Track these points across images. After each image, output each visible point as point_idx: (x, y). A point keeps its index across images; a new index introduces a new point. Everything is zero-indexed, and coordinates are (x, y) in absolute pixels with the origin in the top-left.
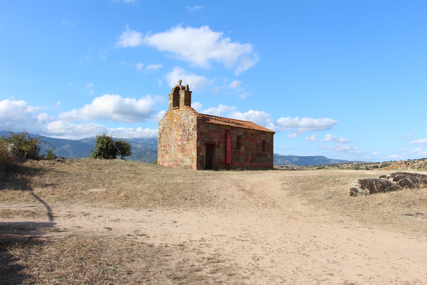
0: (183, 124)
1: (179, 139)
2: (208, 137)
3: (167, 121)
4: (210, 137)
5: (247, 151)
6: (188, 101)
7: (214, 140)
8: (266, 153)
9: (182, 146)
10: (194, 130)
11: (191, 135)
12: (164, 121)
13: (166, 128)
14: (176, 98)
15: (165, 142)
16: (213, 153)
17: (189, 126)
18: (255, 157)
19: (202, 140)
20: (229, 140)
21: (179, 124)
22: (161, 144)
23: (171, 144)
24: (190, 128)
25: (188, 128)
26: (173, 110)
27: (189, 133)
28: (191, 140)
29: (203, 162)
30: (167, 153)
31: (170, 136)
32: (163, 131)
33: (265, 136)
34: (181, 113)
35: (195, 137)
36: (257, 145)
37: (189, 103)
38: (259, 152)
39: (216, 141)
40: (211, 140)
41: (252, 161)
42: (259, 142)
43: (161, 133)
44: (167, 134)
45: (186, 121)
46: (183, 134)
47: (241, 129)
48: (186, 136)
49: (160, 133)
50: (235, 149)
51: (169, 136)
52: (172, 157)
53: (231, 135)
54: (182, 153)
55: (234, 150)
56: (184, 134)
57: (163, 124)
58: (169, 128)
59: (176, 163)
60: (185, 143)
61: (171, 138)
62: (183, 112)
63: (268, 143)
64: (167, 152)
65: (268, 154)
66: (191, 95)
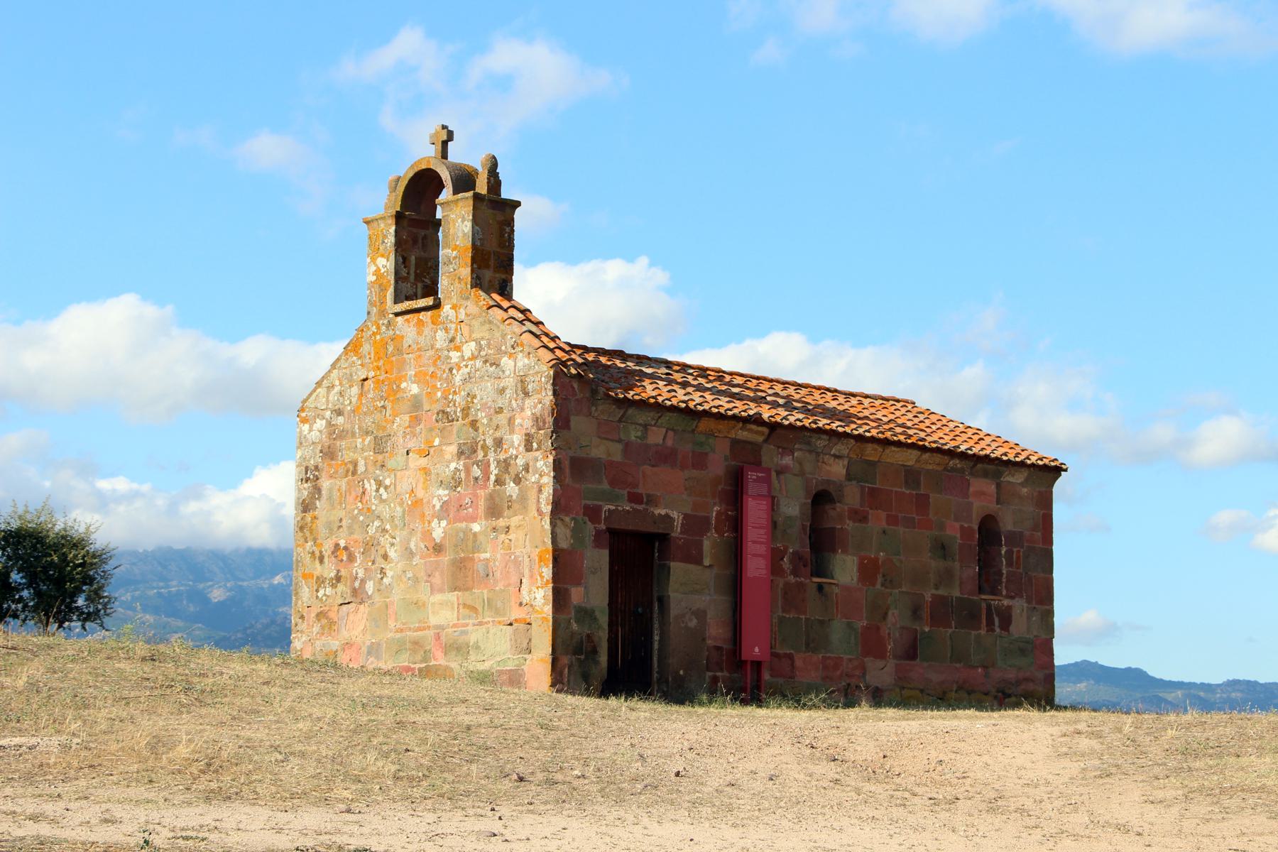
0: (466, 411)
1: (438, 507)
2: (625, 492)
3: (355, 390)
4: (639, 491)
5: (878, 586)
6: (492, 263)
7: (663, 512)
8: (1006, 602)
9: (456, 546)
10: (535, 445)
11: (517, 480)
12: (337, 389)
13: (353, 435)
14: (415, 241)
15: (344, 523)
16: (655, 595)
17: (502, 419)
18: (927, 629)
19: (587, 508)
20: (755, 511)
21: (437, 407)
22: (315, 540)
23: (385, 541)
24: (512, 432)
25: (498, 434)
26: (399, 319)
27: (505, 465)
28: (516, 506)
29: (595, 651)
30: (358, 595)
31: (379, 484)
32: (329, 454)
33: (993, 487)
34: (452, 340)
35: (540, 491)
36: (942, 549)
37: (503, 276)
38: (956, 593)
39: (675, 515)
40: (640, 507)
41: (911, 652)
42: (953, 531)
43: (316, 468)
44: (354, 473)
45: (485, 392)
46: (463, 475)
47: (834, 439)
48: (485, 487)
49: (307, 469)
50: (795, 572)
51: (370, 486)
52: (391, 624)
53: (767, 480)
54: (453, 597)
55: (792, 579)
56: (468, 470)
57: (328, 414)
58: (367, 433)
59: (419, 657)
60: (476, 527)
61: (382, 501)
62: (465, 329)
63: (1015, 539)
64: (355, 592)
65: (1019, 606)
66: (510, 223)
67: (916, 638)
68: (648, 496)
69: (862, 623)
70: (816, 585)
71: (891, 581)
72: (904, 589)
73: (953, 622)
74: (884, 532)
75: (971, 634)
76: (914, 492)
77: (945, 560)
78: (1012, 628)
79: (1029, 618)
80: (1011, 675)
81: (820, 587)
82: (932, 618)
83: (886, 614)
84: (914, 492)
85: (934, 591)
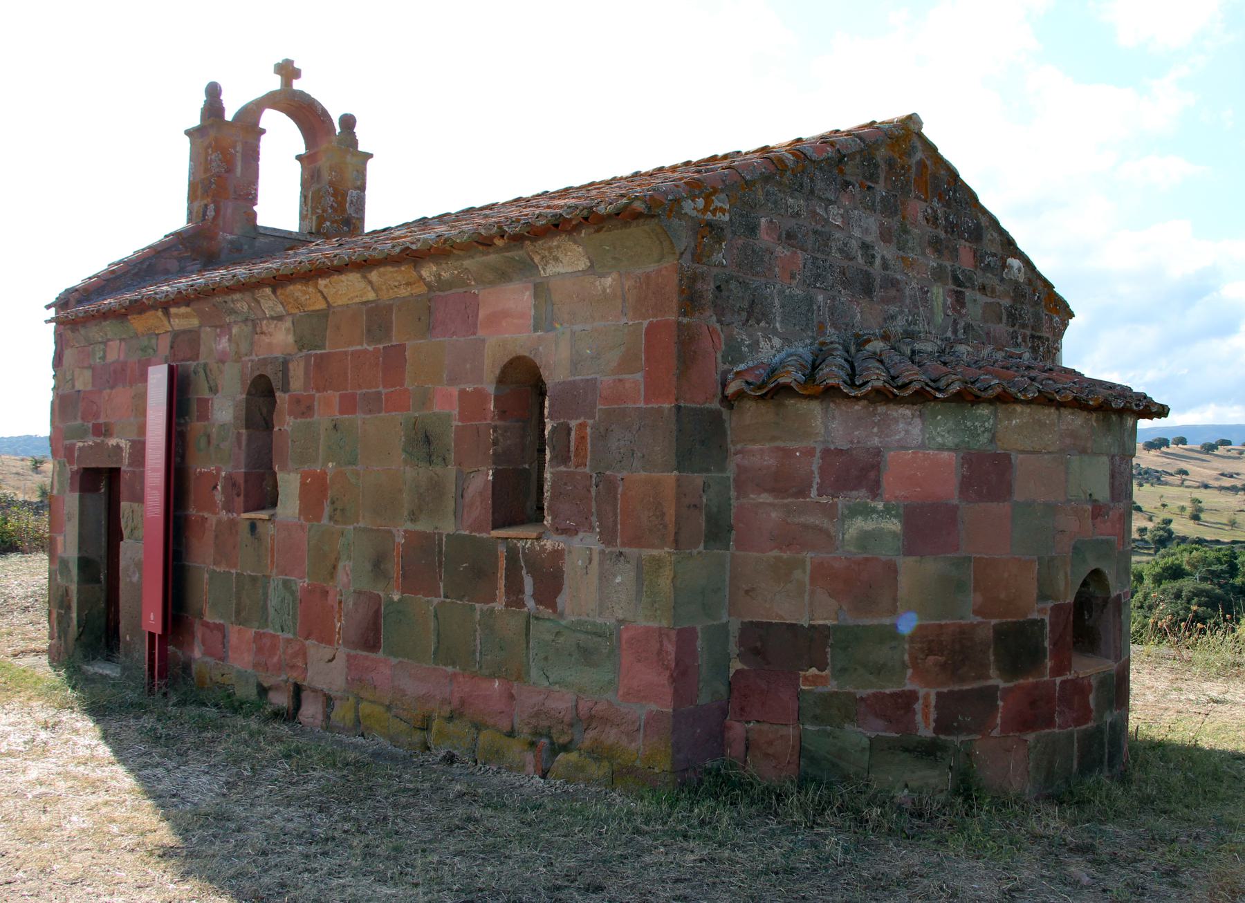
18: (396, 597)
33: (528, 296)
38: (448, 527)
41: (370, 638)
67: (377, 613)
68: (106, 424)
69: (302, 583)
70: (248, 523)
71: (343, 510)
72: (362, 524)
73: (441, 585)
74: (335, 426)
75: (473, 609)
76: (381, 346)
77: (430, 462)
78: (563, 600)
79: (604, 578)
80: (561, 703)
81: (253, 526)
82: (404, 576)
83: (335, 567)
84: (381, 346)
85: (409, 526)
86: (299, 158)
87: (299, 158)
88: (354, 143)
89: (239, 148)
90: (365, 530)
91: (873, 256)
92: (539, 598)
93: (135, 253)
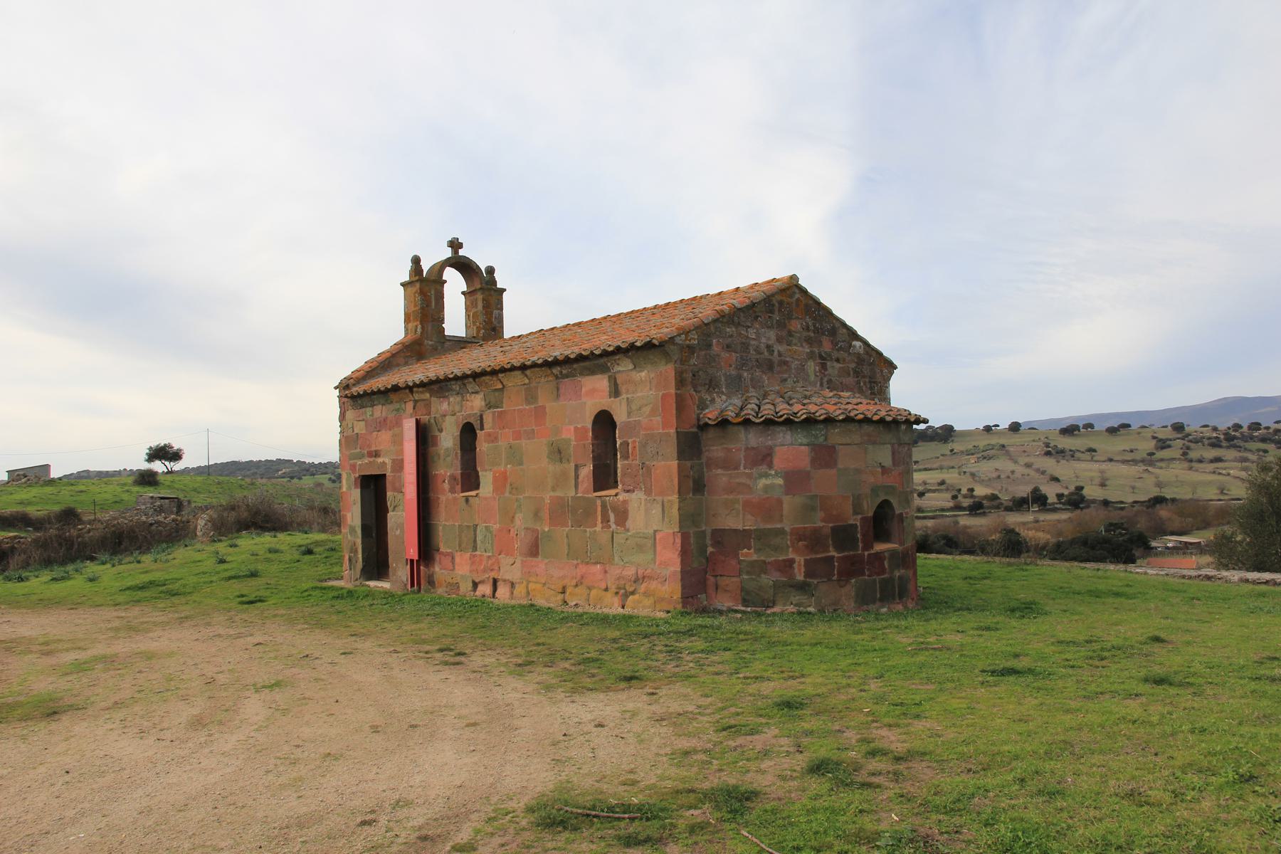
5: (507, 494)
18: (546, 529)
42: (568, 434)
55: (450, 496)
67: (537, 537)
68: (376, 451)
75: (586, 531)
77: (561, 462)
78: (629, 524)
79: (647, 511)
82: (550, 519)
83: (513, 517)
85: (552, 494)
86: (463, 293)
87: (463, 293)
88: (495, 283)
89: (433, 292)
90: (530, 497)
91: (773, 351)
92: (617, 523)
93: (380, 355)
